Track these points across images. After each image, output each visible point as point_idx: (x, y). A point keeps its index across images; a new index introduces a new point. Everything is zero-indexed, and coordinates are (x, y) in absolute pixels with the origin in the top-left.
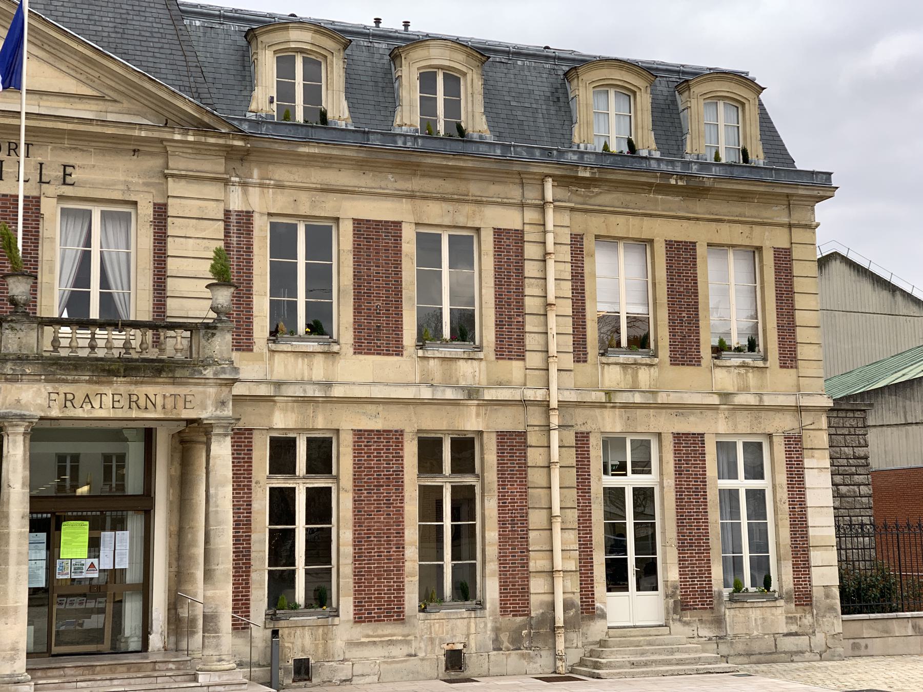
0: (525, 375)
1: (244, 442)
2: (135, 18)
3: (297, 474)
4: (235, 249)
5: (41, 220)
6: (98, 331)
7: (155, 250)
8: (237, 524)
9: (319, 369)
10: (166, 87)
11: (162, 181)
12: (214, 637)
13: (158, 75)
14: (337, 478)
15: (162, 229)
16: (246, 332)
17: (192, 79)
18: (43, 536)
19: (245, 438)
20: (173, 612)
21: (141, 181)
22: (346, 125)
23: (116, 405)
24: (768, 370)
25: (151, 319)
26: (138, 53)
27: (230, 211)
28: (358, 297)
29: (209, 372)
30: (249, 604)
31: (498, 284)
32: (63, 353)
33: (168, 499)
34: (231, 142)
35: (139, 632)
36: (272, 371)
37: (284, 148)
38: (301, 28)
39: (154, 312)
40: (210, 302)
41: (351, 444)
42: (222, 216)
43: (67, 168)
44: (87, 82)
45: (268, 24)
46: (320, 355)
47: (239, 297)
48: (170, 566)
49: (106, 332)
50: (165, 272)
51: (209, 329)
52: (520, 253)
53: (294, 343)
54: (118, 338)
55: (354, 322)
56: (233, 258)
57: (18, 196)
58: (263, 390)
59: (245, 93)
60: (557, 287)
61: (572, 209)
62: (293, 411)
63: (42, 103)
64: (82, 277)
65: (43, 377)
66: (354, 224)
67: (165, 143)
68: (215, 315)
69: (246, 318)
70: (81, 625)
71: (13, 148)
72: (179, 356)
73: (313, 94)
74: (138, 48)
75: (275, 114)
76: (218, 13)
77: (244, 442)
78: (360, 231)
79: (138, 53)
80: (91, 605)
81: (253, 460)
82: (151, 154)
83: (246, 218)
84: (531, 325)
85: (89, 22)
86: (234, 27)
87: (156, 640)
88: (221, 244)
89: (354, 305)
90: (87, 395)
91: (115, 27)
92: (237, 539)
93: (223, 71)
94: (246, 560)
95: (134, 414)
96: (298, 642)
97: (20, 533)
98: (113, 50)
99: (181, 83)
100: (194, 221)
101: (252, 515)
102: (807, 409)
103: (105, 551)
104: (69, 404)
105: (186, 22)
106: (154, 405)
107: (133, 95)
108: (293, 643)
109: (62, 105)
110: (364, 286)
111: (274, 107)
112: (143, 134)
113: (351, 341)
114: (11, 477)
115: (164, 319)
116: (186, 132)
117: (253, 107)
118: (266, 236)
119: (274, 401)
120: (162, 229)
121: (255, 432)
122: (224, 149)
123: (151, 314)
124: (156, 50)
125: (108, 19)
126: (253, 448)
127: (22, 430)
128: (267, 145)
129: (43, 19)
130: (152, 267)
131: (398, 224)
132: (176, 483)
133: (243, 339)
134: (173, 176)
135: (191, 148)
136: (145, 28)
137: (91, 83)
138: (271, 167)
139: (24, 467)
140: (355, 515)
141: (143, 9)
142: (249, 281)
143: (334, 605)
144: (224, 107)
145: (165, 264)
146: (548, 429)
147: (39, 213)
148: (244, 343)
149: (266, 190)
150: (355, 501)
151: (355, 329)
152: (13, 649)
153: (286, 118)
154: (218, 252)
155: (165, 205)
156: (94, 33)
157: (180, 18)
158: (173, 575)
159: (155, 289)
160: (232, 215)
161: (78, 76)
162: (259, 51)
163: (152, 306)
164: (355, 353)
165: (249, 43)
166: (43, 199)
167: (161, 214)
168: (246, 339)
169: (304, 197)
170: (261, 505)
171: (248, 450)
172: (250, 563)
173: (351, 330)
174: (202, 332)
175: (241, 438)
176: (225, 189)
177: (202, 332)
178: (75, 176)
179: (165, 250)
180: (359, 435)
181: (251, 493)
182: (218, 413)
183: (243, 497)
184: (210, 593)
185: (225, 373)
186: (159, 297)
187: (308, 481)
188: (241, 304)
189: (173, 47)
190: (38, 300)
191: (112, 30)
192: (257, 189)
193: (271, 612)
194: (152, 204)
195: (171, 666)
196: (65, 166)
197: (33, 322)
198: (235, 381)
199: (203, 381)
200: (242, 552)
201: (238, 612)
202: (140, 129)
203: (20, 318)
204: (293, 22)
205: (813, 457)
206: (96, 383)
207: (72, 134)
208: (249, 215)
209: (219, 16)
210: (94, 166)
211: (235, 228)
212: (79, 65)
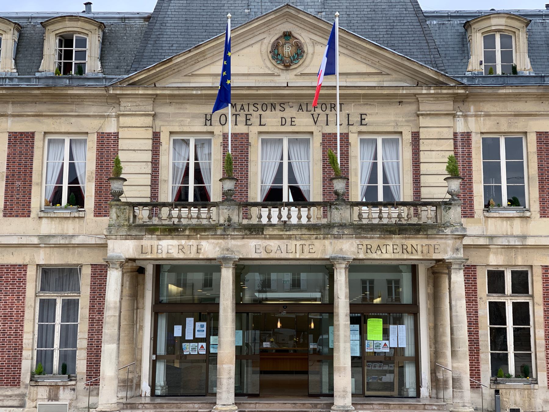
1: (471, 273)
2: (398, 24)
3: (506, 293)
4: (461, 156)
5: (350, 146)
6: (383, 209)
7: (413, 159)
8: (470, 324)
9: (517, 227)
10: (417, 63)
11: (416, 118)
12: (459, 392)
13: (412, 56)
14: (532, 296)
15: (417, 147)
16: (470, 206)
17: (432, 56)
18: (357, 327)
19: (472, 271)
20: (434, 375)
21: (404, 120)
22: (529, 73)
23: (395, 251)
25: (412, 200)
26: (401, 45)
27: (457, 133)
28: (541, 181)
29: (448, 231)
30: (480, 373)
32: (365, 222)
33: (427, 307)
34: (456, 91)
35: (414, 386)
36: (487, 229)
37: (490, 91)
38: (499, 17)
39: (414, 196)
40: (446, 189)
41: (541, 275)
42: (452, 137)
43: (362, 115)
44: (372, 65)
45: (478, 17)
46: (518, 219)
47: (464, 185)
48: (430, 347)
49: (388, 209)
50: (419, 172)
51: (447, 205)
53: (500, 212)
54: (394, 212)
55: (540, 197)
56: (460, 161)
57: (337, 134)
58: (482, 241)
59: (464, 61)
62: (501, 254)
63: (348, 80)
64: (373, 178)
65: (354, 236)
66: (537, 135)
67: (417, 96)
68: (450, 197)
69: (469, 198)
70: (381, 379)
71: (333, 107)
72: (430, 222)
73: (507, 56)
74: (400, 42)
75: (484, 71)
76: (447, 14)
77: (471, 273)
78: (541, 139)
79: (401, 45)
80: (386, 368)
81: (478, 285)
82: (409, 103)
83: (467, 136)
85: (372, 30)
86: (456, 22)
87: (425, 391)
88: (452, 153)
89: (539, 187)
90: (379, 246)
91: (387, 31)
92: (470, 332)
93: (450, 49)
94: (476, 345)
95: (405, 256)
96: (512, 398)
97: (345, 325)
98: (386, 45)
99: (426, 59)
100: (435, 141)
101: (479, 318)
103: (392, 336)
104: (369, 251)
105: (428, 22)
106: (417, 251)
108: (508, 399)
109: (359, 80)
110: (545, 174)
111: (483, 67)
112: (404, 92)
113: (538, 209)
114: (339, 292)
115: (420, 200)
116: (429, 88)
117: (470, 68)
118: (480, 147)
119: (489, 248)
120: (417, 147)
121: (477, 267)
122: (452, 96)
123: (412, 198)
124: (411, 42)
125: (383, 27)
126: (477, 277)
127: (344, 266)
128: (479, 91)
129: (347, 32)
130: (412, 169)
132: (431, 298)
133: (468, 210)
134: (422, 115)
135: (433, 97)
136: (404, 30)
137: (374, 66)
138: (481, 104)
139: (346, 287)
140: (546, 320)
141: (403, 18)
142: (470, 175)
143: (534, 376)
144: (452, 70)
145: (419, 168)
147: (348, 142)
148: (468, 213)
149: (479, 119)
150: (545, 311)
151: (540, 201)
152: (344, 391)
153: (491, 73)
154: (450, 158)
155: (418, 133)
156: (375, 36)
157: (424, 21)
158: (432, 353)
159: (414, 183)
160: (458, 135)
161: (367, 62)
162: (473, 34)
163: (412, 192)
164: (541, 217)
165: (466, 30)
166: (350, 135)
167: (416, 138)
168: (470, 210)
170: (484, 313)
171: (474, 278)
172: (479, 348)
173: (538, 202)
174: (443, 207)
175: (469, 271)
176: (454, 120)
177: (443, 207)
178: (368, 119)
179: (419, 159)
180: (546, 269)
181: (477, 305)
182: (455, 255)
183: (472, 307)
184: (455, 365)
185: (458, 231)
186: (417, 187)
187: (513, 298)
188: (466, 189)
189: (420, 38)
190: (350, 192)
191: (385, 33)
192: (474, 118)
193: (493, 378)
194: (410, 133)
195: (434, 407)
196: (361, 115)
197: (347, 205)
198: (464, 236)
199: (445, 236)
200: (474, 341)
201: (473, 378)
202: (403, 89)
203: (340, 202)
204: (493, 14)
206: (383, 238)
207: (365, 96)
208: (469, 134)
209: (448, 16)
210: (377, 113)
211: (460, 143)
212: (367, 56)
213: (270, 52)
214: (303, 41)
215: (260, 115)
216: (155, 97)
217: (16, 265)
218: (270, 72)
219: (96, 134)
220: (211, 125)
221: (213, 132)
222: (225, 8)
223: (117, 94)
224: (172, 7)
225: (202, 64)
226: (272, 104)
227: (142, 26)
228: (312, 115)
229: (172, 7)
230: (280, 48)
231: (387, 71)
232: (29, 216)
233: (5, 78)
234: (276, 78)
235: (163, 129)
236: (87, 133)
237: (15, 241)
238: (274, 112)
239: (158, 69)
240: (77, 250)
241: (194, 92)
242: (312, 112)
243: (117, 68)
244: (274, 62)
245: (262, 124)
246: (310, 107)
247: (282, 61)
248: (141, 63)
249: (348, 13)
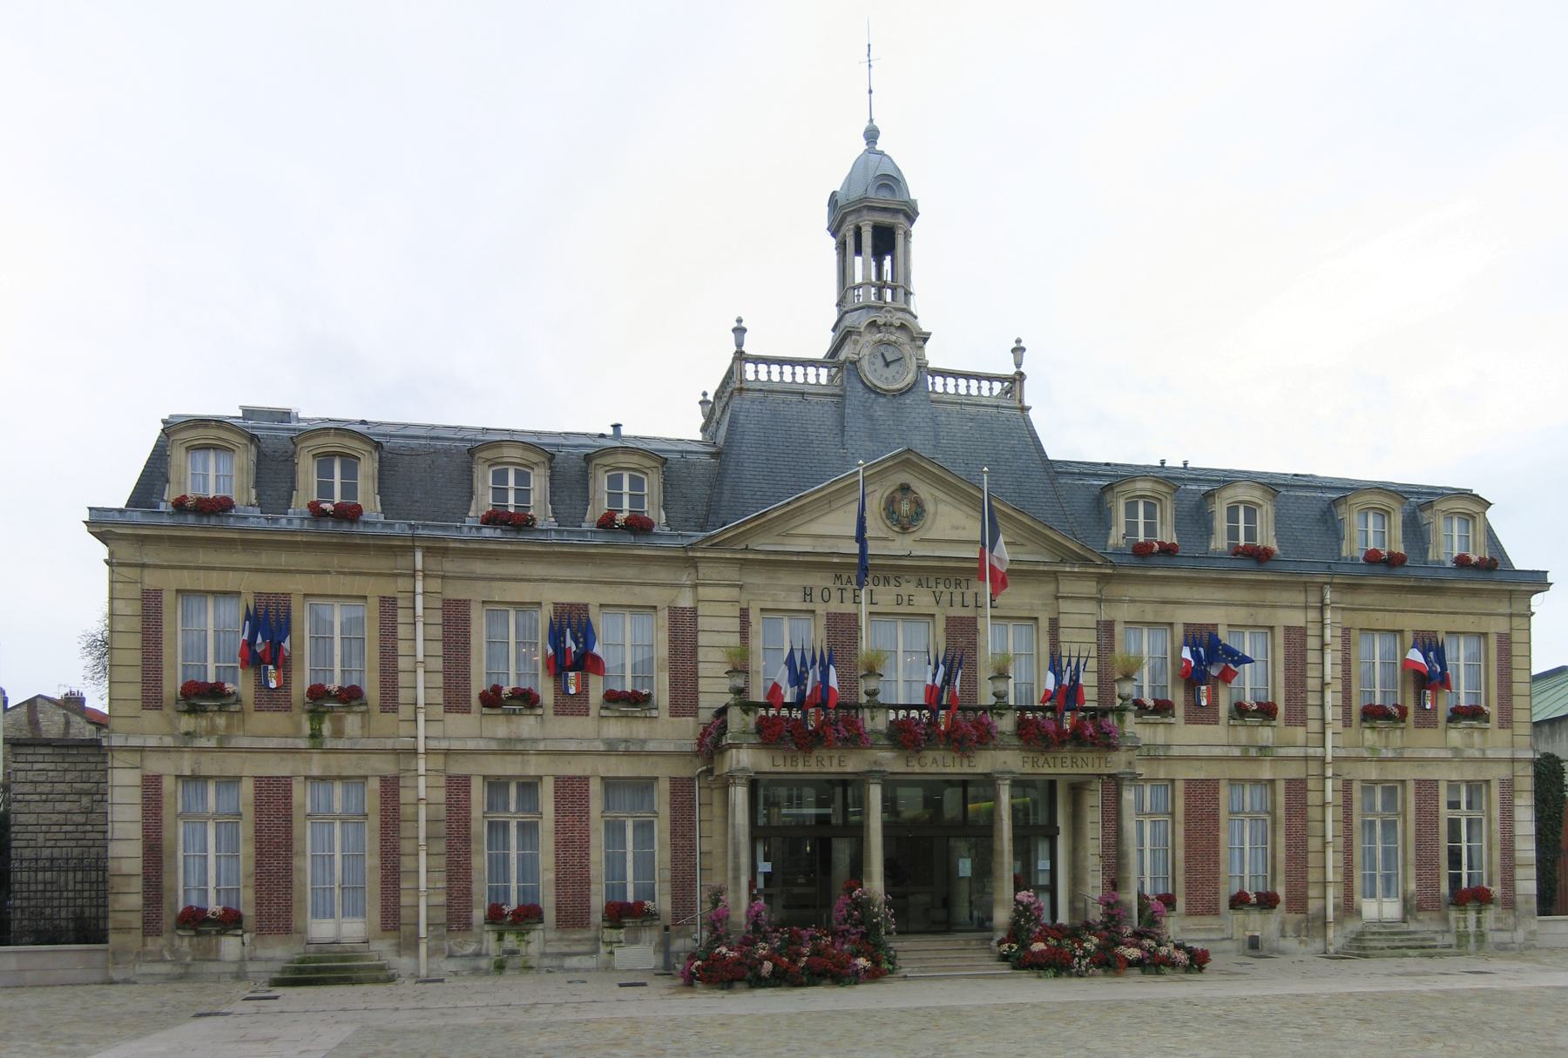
0: (1307, 738)
11: (1055, 602)
21: (1040, 602)
24: (1489, 731)
31: (1287, 669)
34: (1103, 571)
84: (1313, 699)
102: (1519, 760)
107: (1035, 540)
116: (1073, 565)
146: (1324, 778)
157: (1055, 478)
167: (1054, 626)
169: (1149, 608)
173: (1183, 707)
205: (1521, 797)
210: (1010, 593)
213: (884, 509)
214: (922, 497)
215: (871, 591)
216: (742, 562)
217: (574, 777)
218: (883, 536)
219: (667, 609)
220: (811, 601)
221: (813, 612)
222: (814, 445)
223: (693, 558)
224: (747, 441)
225: (797, 521)
226: (885, 578)
228: (934, 592)
229: (747, 441)
231: (1020, 540)
232: (587, 715)
233: (550, 530)
234: (890, 544)
235: (752, 604)
236: (655, 607)
237: (573, 746)
238: (887, 587)
239: (748, 526)
240: (651, 760)
241: (795, 558)
242: (934, 589)
243: (686, 521)
244: (887, 522)
245: (873, 602)
246: (932, 583)
247: (898, 522)
248: (720, 516)
249: (966, 461)
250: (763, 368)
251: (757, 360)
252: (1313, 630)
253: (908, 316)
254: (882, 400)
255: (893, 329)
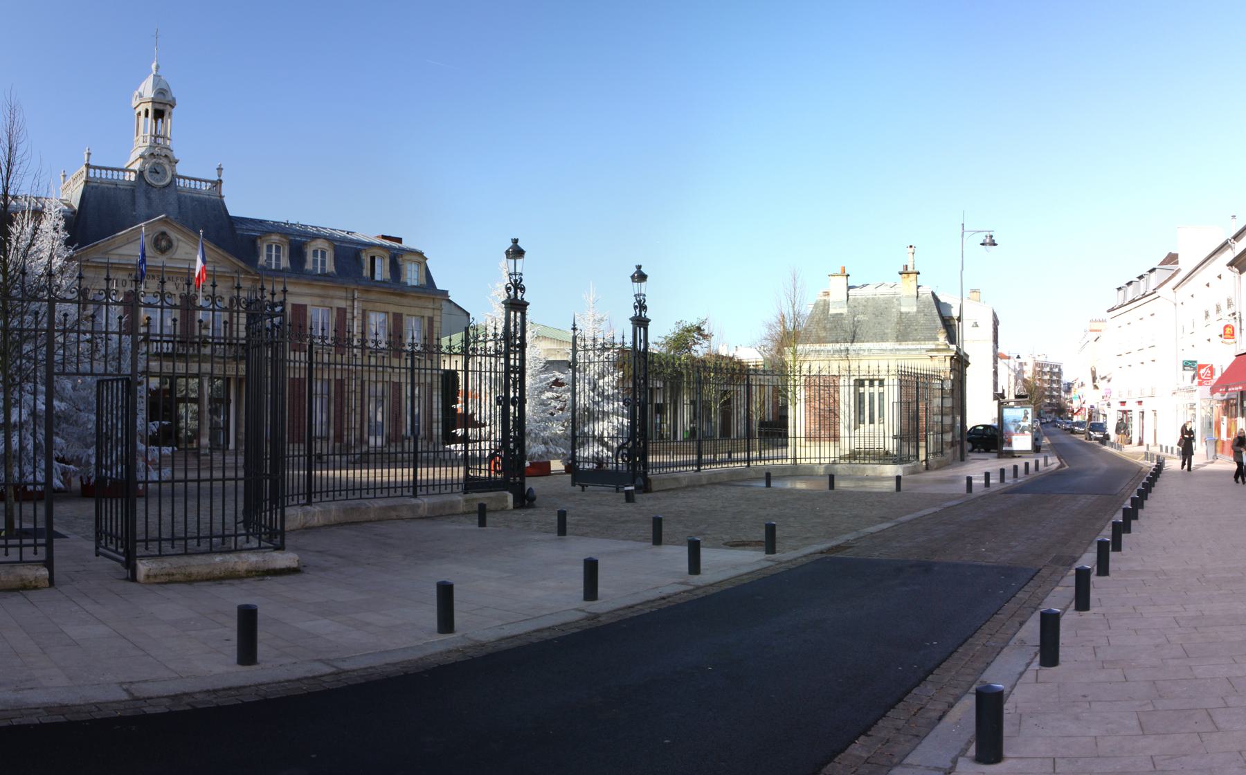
34: (255, 277)
52: (345, 316)
60: (357, 329)
61: (363, 301)
131: (306, 306)
227: (70, 217)
230: (159, 242)
250: (98, 171)
251: (95, 168)
252: (349, 310)
253: (169, 151)
254: (155, 190)
255: (162, 158)
